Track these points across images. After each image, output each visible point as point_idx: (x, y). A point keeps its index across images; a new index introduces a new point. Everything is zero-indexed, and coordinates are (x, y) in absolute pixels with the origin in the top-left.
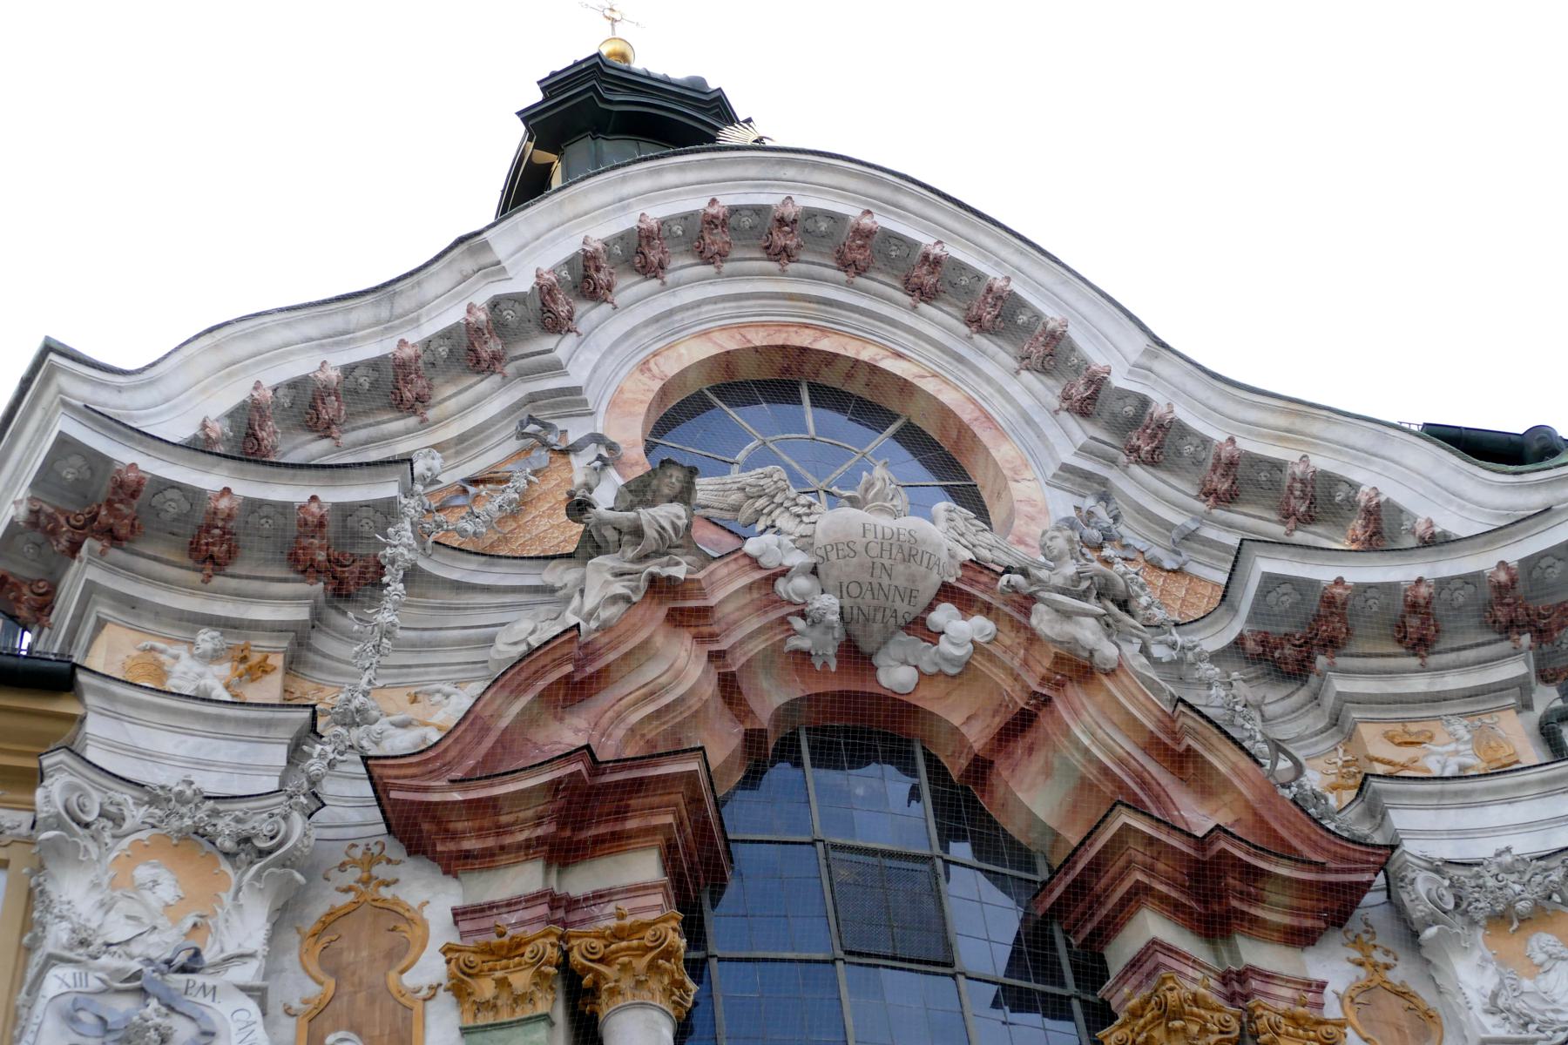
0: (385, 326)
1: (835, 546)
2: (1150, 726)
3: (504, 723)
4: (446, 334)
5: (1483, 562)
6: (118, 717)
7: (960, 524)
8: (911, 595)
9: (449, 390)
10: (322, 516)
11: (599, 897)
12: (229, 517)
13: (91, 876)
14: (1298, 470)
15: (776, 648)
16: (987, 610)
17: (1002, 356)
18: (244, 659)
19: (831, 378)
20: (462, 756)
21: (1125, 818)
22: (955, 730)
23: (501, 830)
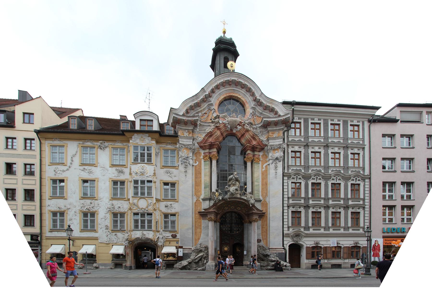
8: (235, 125)
16: (241, 126)
18: (189, 132)
23: (206, 147)
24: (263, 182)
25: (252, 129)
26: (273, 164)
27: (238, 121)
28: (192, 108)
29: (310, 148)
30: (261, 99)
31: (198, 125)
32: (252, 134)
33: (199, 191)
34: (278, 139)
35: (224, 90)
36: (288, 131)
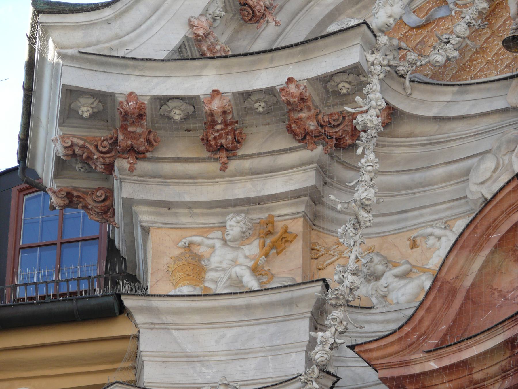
3: (468, 282)
6: (166, 327)
10: (301, 94)
12: (224, 113)
20: (435, 323)
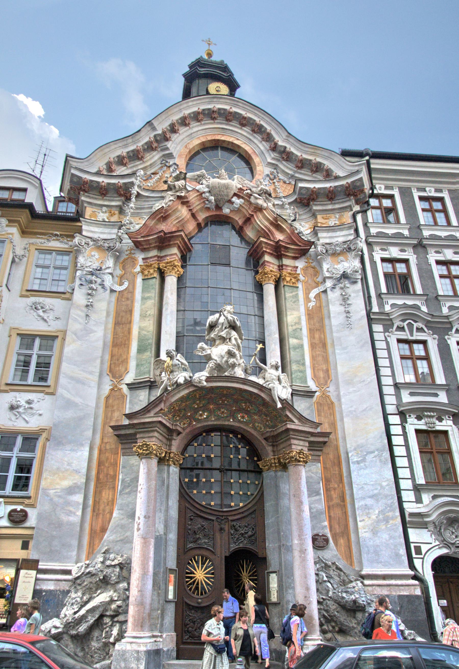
0: (134, 142)
1: (213, 187)
2: (271, 219)
4: (146, 143)
5: (343, 182)
7: (240, 180)
8: (228, 196)
9: (148, 154)
11: (166, 256)
13: (82, 255)
14: (314, 161)
15: (203, 207)
16: (243, 198)
17: (259, 138)
19: (225, 145)
20: (143, 232)
21: (262, 239)
22: (236, 221)
23: (150, 244)
24: (314, 338)
25: (270, 205)
26: (335, 290)
27: (234, 188)
28: (121, 161)
29: (429, 252)
30: (288, 146)
31: (132, 196)
32: (271, 217)
33: (122, 362)
34: (341, 230)
35: (200, 128)
36: (364, 212)
